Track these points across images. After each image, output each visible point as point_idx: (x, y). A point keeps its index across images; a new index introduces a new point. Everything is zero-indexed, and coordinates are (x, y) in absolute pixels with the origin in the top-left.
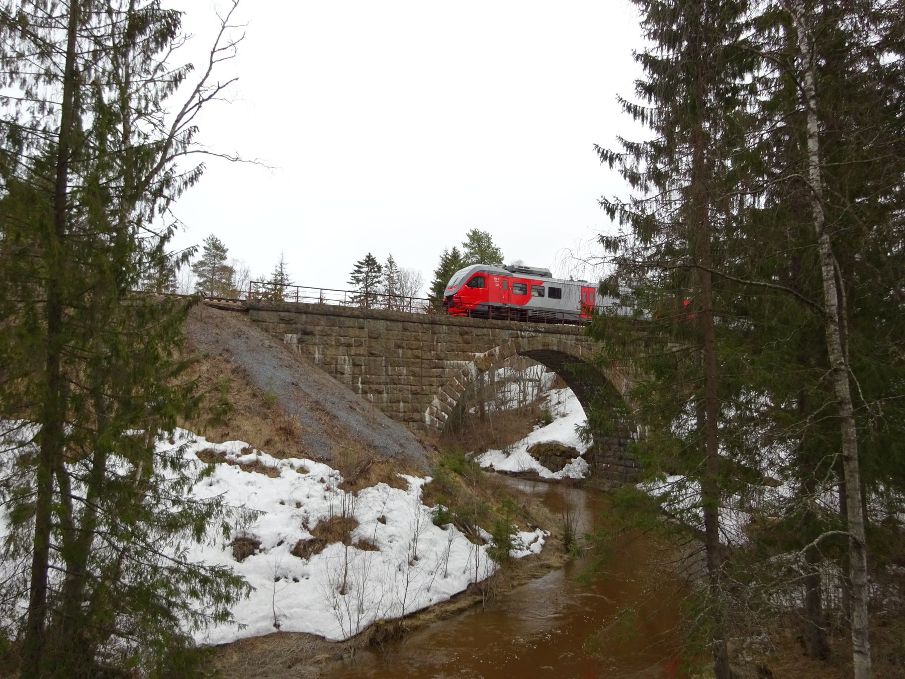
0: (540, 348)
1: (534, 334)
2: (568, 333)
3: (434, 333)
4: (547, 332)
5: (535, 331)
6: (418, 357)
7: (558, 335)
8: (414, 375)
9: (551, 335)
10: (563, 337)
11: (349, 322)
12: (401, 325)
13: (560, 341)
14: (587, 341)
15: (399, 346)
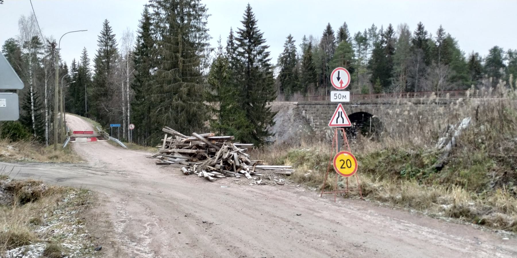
0: (359, 111)
1: (356, 105)
2: (368, 104)
3: (330, 108)
4: (361, 104)
5: (357, 104)
6: (325, 116)
7: (365, 105)
8: (325, 122)
9: (363, 105)
10: (367, 105)
11: (313, 106)
12: (322, 106)
13: (366, 108)
14: (376, 106)
15: (322, 113)
